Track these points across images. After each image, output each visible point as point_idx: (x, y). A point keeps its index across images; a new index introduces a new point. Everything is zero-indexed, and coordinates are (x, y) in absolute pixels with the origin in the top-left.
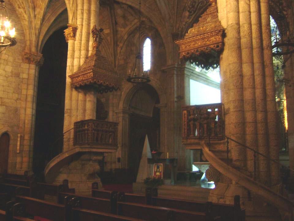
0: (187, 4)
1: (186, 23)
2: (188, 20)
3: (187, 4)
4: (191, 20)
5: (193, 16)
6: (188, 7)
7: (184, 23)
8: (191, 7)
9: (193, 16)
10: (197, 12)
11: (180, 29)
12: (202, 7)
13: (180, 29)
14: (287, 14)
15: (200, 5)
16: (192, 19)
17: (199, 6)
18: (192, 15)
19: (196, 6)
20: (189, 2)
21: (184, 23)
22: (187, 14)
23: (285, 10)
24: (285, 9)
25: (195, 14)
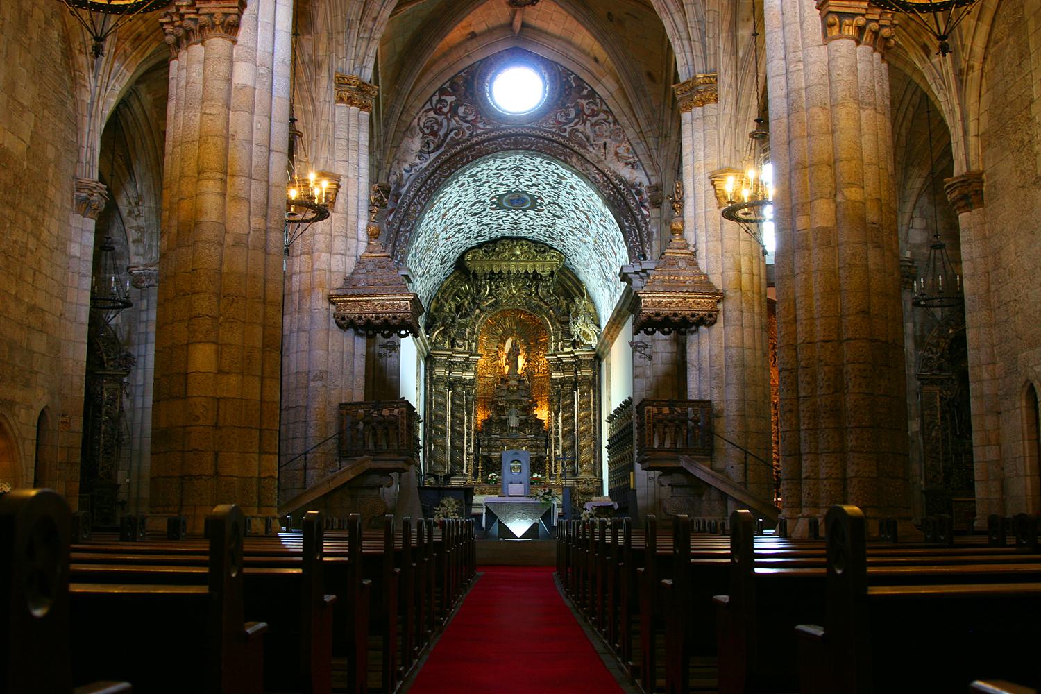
0: (416, 120)
1: (411, 167)
2: (418, 161)
3: (416, 120)
4: (425, 165)
5: (433, 156)
6: (418, 129)
7: (407, 166)
8: (427, 131)
9: (433, 156)
10: (442, 149)
11: (393, 178)
12: (458, 143)
13: (393, 178)
14: (649, 216)
15: (452, 134)
16: (428, 162)
18: (429, 153)
19: (441, 133)
20: (423, 120)
21: (407, 166)
22: (416, 144)
23: (645, 207)
24: (646, 204)
25: (439, 152)
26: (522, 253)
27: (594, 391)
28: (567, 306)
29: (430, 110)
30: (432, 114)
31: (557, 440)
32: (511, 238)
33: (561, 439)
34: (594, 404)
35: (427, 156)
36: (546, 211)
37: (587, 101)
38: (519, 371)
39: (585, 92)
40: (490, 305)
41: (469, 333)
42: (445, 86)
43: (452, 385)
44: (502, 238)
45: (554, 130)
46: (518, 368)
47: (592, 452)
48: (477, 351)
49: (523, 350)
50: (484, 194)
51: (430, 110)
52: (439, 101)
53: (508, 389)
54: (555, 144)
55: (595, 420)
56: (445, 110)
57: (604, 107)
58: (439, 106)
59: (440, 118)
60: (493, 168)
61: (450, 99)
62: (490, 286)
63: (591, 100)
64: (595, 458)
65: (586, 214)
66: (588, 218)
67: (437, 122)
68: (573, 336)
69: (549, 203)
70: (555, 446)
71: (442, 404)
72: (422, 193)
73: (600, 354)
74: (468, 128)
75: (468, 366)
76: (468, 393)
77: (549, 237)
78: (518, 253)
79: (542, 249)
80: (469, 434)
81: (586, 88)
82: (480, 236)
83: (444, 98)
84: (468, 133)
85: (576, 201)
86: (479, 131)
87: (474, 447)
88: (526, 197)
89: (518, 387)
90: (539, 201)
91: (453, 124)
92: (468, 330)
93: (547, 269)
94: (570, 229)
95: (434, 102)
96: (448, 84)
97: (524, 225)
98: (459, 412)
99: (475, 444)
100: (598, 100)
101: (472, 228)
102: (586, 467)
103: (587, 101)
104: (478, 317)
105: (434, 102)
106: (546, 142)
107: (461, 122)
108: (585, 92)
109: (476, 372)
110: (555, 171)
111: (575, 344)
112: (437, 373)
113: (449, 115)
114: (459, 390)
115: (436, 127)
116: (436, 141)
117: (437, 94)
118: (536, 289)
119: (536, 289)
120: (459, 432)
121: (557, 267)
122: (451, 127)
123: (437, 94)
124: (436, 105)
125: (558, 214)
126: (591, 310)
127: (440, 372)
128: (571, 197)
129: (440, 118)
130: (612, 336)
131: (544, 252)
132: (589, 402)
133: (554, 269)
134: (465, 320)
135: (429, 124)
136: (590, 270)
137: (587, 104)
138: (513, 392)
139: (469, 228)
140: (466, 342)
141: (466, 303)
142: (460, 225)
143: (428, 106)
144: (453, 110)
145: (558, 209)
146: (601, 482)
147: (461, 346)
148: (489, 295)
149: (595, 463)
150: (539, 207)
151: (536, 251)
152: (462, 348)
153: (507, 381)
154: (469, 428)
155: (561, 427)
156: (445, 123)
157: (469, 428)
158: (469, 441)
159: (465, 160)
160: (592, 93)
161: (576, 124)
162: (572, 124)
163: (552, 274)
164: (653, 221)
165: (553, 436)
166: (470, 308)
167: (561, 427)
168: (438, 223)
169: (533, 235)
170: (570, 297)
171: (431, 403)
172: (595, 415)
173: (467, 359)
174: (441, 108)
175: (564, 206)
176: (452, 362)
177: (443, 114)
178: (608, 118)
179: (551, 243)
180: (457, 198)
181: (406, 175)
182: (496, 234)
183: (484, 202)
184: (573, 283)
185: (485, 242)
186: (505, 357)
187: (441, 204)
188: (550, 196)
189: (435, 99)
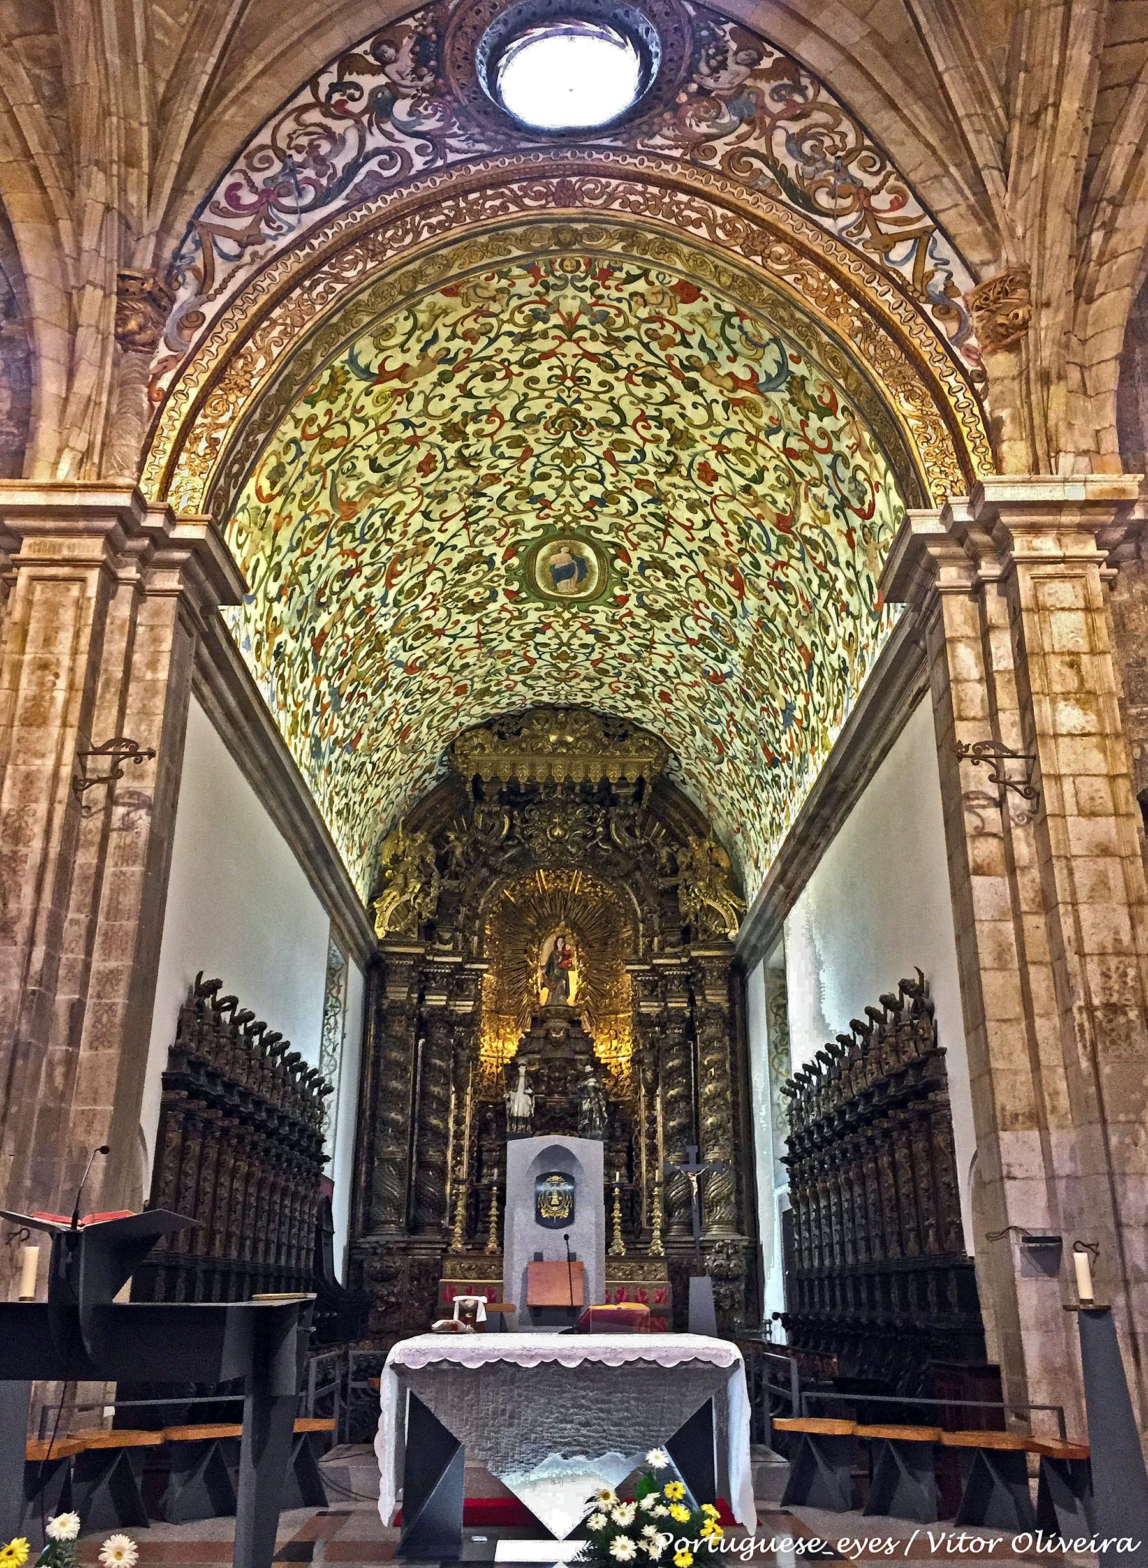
15: (373, 165)
17: (363, 172)
19: (340, 162)
26: (577, 740)
27: (733, 1040)
28: (672, 858)
29: (306, 108)
30: (314, 116)
31: (652, 1150)
32: (553, 708)
33: (660, 1148)
34: (734, 1067)
35: (292, 219)
36: (632, 603)
37: (774, 84)
38: (571, 1001)
39: (766, 63)
40: (511, 860)
41: (467, 917)
42: (359, 50)
43: (423, 1026)
44: (539, 706)
45: (677, 153)
46: (567, 993)
47: (732, 1176)
48: (481, 953)
49: (579, 958)
50: (490, 530)
51: (306, 108)
52: (333, 88)
53: (547, 1037)
54: (682, 197)
55: (735, 1105)
56: (355, 107)
57: (824, 96)
58: (336, 97)
59: (337, 126)
60: (505, 409)
61: (369, 82)
62: (511, 819)
63: (786, 81)
64: (739, 1191)
65: (731, 569)
66: (738, 585)
67: (329, 134)
68: (687, 915)
69: (644, 566)
70: (649, 1164)
71: (397, 1064)
72: (274, 323)
73: (745, 955)
74: (420, 150)
75: (460, 985)
76: (460, 1043)
77: (638, 696)
78: (570, 739)
79: (621, 731)
80: (459, 1135)
81: (771, 54)
82: (486, 692)
83: (347, 78)
84: (419, 163)
85: (715, 531)
86: (452, 157)
87: (471, 1166)
88: (588, 552)
89: (567, 1032)
90: (619, 564)
91: (375, 140)
92: (463, 910)
93: (632, 775)
94: (686, 649)
95: (323, 91)
96: (366, 46)
97: (585, 667)
98: (437, 1084)
99: (471, 1157)
100: (805, 81)
101: (471, 659)
102: (720, 1212)
103: (774, 84)
104: (484, 884)
105: (323, 91)
106: (654, 190)
107: (398, 136)
108: (766, 63)
109: (477, 998)
110: (669, 411)
111: (687, 936)
112: (392, 997)
113: (365, 119)
114: (440, 1033)
115: (325, 147)
116: (324, 181)
117: (334, 68)
118: (606, 826)
119: (606, 826)
120: (435, 1130)
121: (651, 769)
122: (370, 145)
123: (334, 68)
124: (329, 97)
125: (661, 603)
126: (724, 864)
127: (398, 993)
128: (698, 518)
129: (337, 126)
130: (789, 887)
131: (624, 736)
132: (723, 1062)
133: (646, 774)
134: (454, 883)
135: (304, 141)
136: (725, 767)
137: (775, 91)
138: (557, 1044)
139: (462, 653)
140: (459, 936)
141: (458, 852)
142: (440, 633)
143: (306, 97)
144: (381, 108)
145: (662, 584)
146: (754, 1254)
147: (446, 943)
148: (509, 837)
149: (738, 1204)
150: (618, 591)
151: (607, 735)
152: (449, 947)
153: (543, 1021)
154: (459, 1121)
155: (660, 1119)
156: (352, 137)
157: (459, 1121)
158: (458, 1151)
159: (408, 239)
160: (791, 64)
161: (742, 138)
162: (731, 138)
163: (641, 781)
164: (995, 390)
165: (643, 1141)
166: (468, 862)
167: (660, 1119)
168: (378, 590)
169: (602, 698)
170: (674, 837)
171: (376, 1063)
172: (735, 1093)
173: (459, 967)
174: (341, 103)
175: (676, 564)
176: (426, 974)
177: (346, 115)
178: (838, 123)
179: (638, 714)
180: (417, 521)
181: (221, 269)
182: (524, 696)
183: (490, 561)
184: (685, 815)
185: (502, 716)
186: (540, 973)
187: (376, 520)
188: (644, 537)
189: (325, 81)
